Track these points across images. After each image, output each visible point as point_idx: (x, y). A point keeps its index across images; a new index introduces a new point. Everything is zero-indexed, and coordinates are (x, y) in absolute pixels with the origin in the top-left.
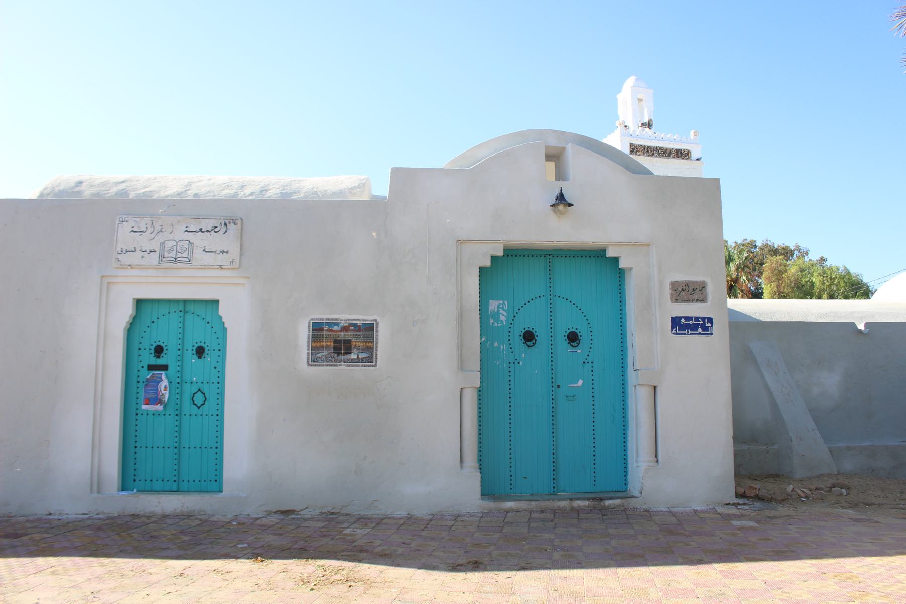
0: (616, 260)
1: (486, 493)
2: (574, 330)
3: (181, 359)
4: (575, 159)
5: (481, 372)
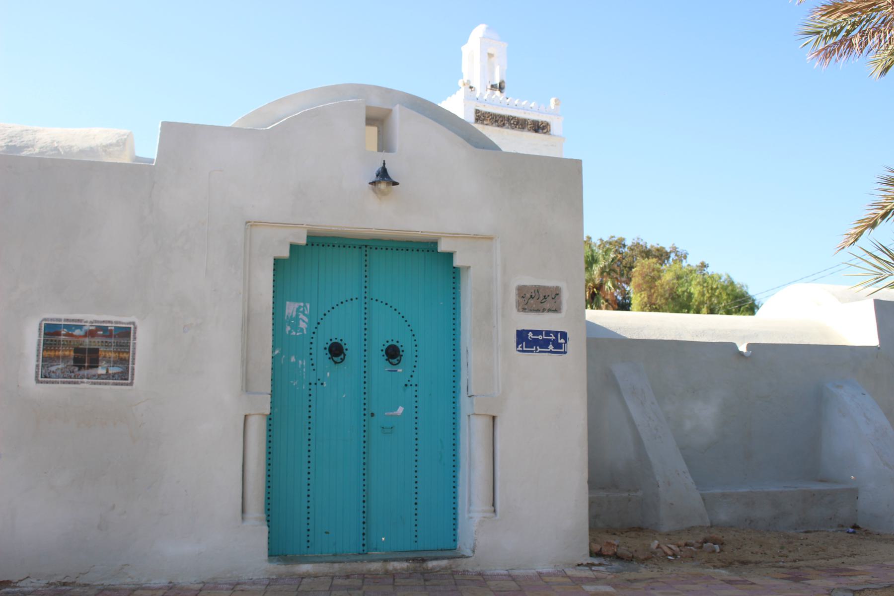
0: (450, 256)
1: (275, 553)
2: (394, 343)
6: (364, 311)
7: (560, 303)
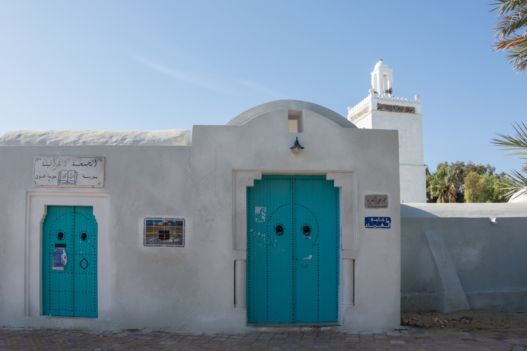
0: (332, 182)
2: (307, 225)
3: (73, 240)
4: (310, 120)
5: (249, 250)
6: (292, 210)
7: (387, 203)
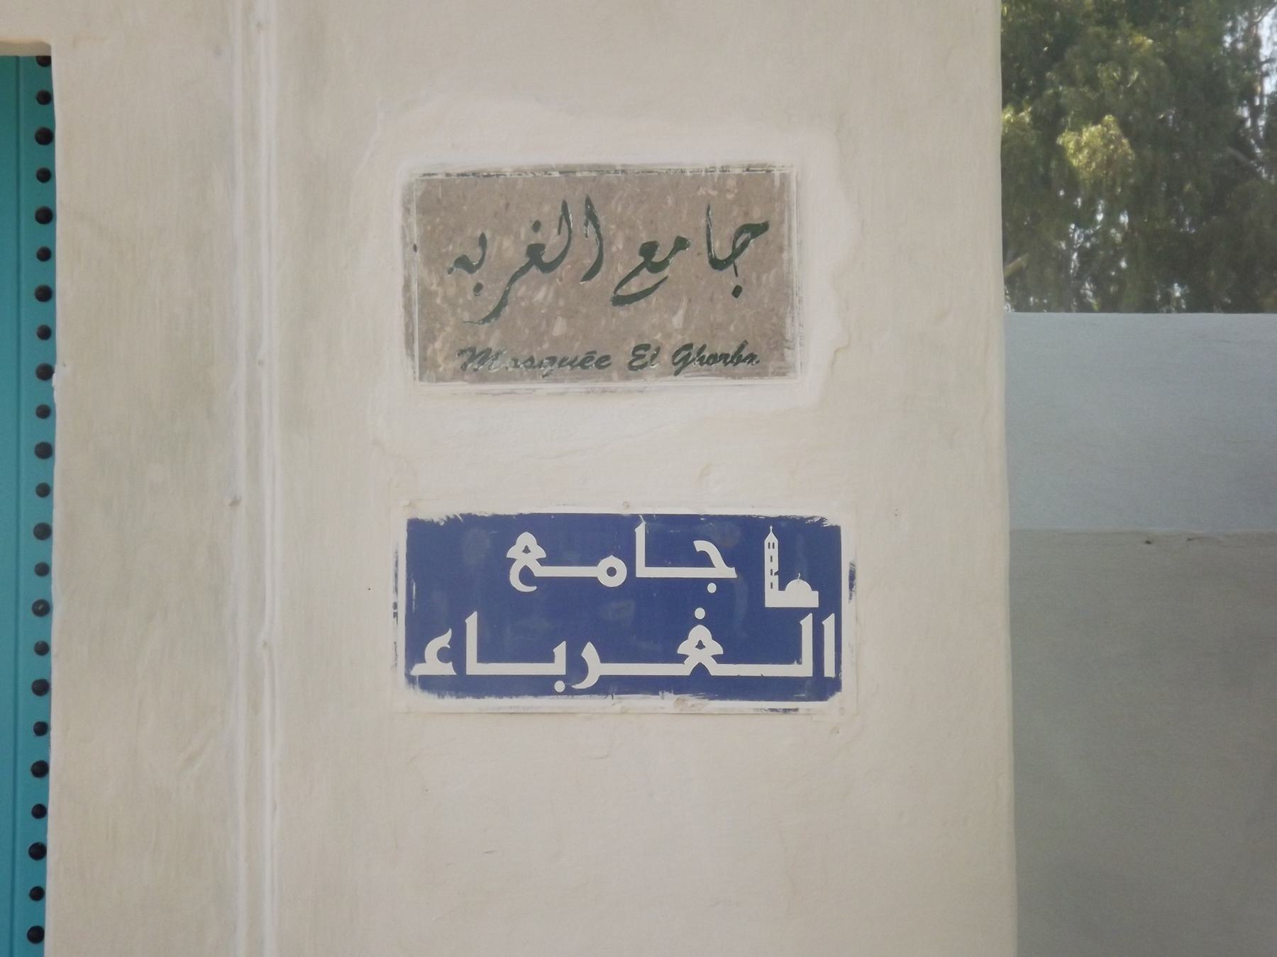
7: (784, 293)
